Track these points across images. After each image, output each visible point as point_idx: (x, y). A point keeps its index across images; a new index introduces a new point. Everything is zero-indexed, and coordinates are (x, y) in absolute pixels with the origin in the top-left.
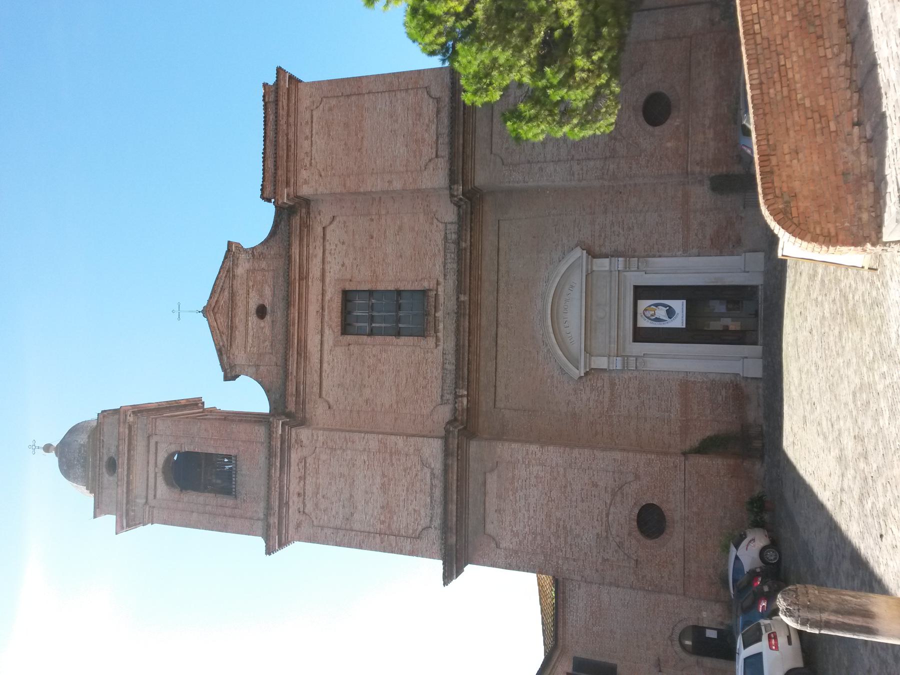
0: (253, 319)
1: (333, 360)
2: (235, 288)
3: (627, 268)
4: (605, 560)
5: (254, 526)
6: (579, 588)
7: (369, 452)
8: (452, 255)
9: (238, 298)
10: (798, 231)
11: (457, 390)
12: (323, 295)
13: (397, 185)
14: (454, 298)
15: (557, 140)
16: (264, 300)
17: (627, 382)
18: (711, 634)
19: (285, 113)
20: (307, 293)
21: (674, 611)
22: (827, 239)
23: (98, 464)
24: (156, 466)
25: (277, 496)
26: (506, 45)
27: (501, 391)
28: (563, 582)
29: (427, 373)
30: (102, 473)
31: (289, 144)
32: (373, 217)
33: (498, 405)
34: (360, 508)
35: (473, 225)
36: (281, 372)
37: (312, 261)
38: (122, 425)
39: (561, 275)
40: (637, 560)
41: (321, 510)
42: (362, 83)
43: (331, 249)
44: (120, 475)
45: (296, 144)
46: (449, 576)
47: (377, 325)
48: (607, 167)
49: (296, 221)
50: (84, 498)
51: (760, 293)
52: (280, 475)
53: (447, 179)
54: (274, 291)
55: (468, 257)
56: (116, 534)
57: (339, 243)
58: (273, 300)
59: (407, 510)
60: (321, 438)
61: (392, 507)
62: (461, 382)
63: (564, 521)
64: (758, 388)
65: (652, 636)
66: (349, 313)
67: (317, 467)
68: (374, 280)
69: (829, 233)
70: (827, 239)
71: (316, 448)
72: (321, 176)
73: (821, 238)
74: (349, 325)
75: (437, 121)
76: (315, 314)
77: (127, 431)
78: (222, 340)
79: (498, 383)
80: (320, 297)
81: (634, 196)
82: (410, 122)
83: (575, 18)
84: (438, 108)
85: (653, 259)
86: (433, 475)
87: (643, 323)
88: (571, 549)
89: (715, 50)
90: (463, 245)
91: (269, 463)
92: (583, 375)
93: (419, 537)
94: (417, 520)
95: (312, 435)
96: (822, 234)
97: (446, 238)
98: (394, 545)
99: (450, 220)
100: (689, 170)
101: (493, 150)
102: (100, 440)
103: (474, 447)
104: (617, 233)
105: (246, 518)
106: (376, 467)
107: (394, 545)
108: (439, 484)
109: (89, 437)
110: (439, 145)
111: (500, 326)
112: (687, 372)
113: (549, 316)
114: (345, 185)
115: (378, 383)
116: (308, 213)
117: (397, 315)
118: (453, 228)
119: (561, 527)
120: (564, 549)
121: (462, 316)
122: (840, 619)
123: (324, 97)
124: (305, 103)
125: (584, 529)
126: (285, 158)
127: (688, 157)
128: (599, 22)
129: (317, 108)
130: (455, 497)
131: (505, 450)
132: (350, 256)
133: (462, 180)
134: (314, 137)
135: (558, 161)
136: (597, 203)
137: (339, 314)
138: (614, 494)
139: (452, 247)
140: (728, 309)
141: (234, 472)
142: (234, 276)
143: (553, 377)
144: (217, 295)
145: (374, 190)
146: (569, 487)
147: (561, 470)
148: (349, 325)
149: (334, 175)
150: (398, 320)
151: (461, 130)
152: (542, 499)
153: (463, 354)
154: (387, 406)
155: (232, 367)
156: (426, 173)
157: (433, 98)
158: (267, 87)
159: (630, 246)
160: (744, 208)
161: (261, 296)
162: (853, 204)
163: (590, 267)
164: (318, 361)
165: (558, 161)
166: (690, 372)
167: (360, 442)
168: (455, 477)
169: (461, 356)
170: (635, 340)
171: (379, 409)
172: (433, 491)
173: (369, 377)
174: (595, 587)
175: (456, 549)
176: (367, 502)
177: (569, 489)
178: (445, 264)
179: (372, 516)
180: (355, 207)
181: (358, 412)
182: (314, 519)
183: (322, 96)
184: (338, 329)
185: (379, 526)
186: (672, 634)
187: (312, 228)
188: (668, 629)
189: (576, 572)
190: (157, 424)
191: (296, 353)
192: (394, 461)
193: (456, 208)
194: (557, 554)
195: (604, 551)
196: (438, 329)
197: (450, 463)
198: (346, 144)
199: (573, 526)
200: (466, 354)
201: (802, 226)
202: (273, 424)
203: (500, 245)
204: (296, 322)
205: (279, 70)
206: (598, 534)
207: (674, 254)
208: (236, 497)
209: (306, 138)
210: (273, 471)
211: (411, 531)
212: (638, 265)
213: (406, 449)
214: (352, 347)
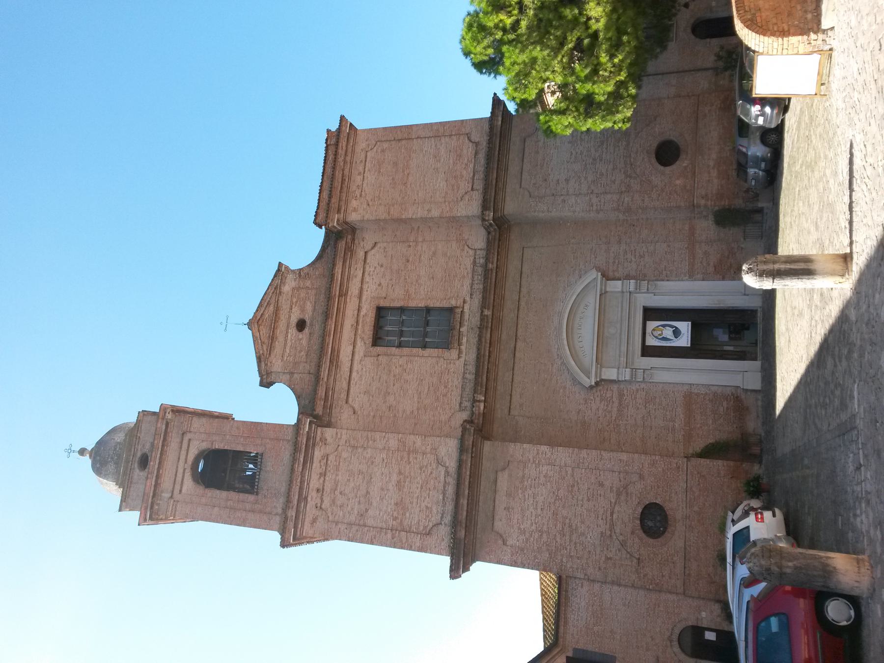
0: (293, 331)
1: (362, 369)
2: (280, 304)
3: (638, 288)
4: (608, 559)
5: (272, 521)
6: (582, 587)
7: (388, 450)
8: (479, 277)
9: (281, 312)
10: (761, 30)
11: (476, 395)
12: (359, 310)
13: (435, 213)
14: (478, 315)
15: (582, 133)
16: (305, 315)
17: (635, 394)
18: (710, 636)
19: (343, 153)
20: (345, 308)
21: (674, 611)
22: (782, 33)
23: (131, 459)
24: (186, 462)
25: (297, 490)
26: (544, 46)
27: (516, 398)
28: (566, 581)
29: (448, 382)
30: (134, 469)
31: (344, 178)
32: (411, 244)
33: (512, 412)
34: (375, 504)
35: (500, 250)
36: (313, 379)
37: (352, 280)
38: (160, 420)
39: (577, 293)
40: (639, 559)
41: (337, 506)
42: (412, 131)
43: (370, 271)
44: (151, 468)
45: (350, 179)
46: (456, 571)
47: (406, 339)
48: (623, 200)
49: (342, 245)
50: (112, 492)
51: (760, 315)
52: (302, 471)
53: (480, 209)
54: (315, 307)
55: (494, 277)
56: (139, 525)
57: (377, 266)
58: (313, 314)
59: (420, 507)
60: (344, 437)
61: (405, 504)
62: (479, 388)
63: (570, 520)
64: (757, 400)
65: (652, 637)
66: (381, 328)
67: (337, 464)
68: (407, 298)
69: (783, 29)
70: (782, 33)
71: (339, 446)
72: (369, 205)
73: (778, 33)
74: (380, 338)
75: (475, 161)
76: (350, 327)
77: (164, 427)
78: (263, 349)
79: (514, 392)
80: (356, 312)
81: (646, 228)
82: (451, 161)
83: (601, 25)
84: (476, 151)
85: (662, 282)
86: (447, 473)
87: (651, 342)
88: (575, 547)
89: (719, 106)
90: (490, 266)
91: (293, 458)
92: (593, 384)
93: (429, 534)
94: (428, 516)
95: (337, 434)
96: (778, 31)
97: (474, 262)
98: (404, 541)
99: (480, 247)
100: (695, 202)
101: (522, 184)
102: (137, 436)
103: (487, 446)
104: (629, 260)
105: (265, 513)
106: (393, 465)
107: (404, 541)
108: (452, 481)
109: (126, 435)
110: (475, 181)
111: (518, 340)
112: (691, 384)
113: (565, 330)
114: (389, 213)
115: (401, 391)
116: (353, 240)
117: (425, 330)
118: (483, 253)
119: (567, 525)
120: (569, 547)
121: (485, 328)
122: (788, 266)
123: (379, 141)
124: (361, 145)
125: (589, 527)
126: (339, 189)
127: (694, 193)
128: (620, 32)
129: (371, 149)
130: (467, 492)
131: (517, 450)
132: (386, 277)
133: (494, 208)
134: (366, 172)
135: (579, 194)
136: (612, 234)
137: (372, 328)
138: (619, 494)
139: (480, 270)
140: (730, 338)
141: (259, 463)
142: (280, 292)
143: (565, 388)
144: (263, 309)
145: (414, 217)
146: (576, 486)
147: (569, 470)
148: (380, 338)
149: (380, 204)
150: (426, 335)
151: (496, 166)
152: (550, 498)
153: (483, 363)
154: (408, 413)
155: (268, 374)
156: (461, 203)
157: (473, 143)
158: (330, 133)
159: (641, 271)
160: (744, 239)
161: (303, 310)
162: (800, 10)
163: (603, 288)
164: (348, 370)
165: (579, 194)
166: (693, 384)
167: (380, 440)
168: (468, 473)
169: (481, 364)
170: (643, 355)
171: (400, 415)
172: (446, 489)
173: (394, 385)
174: (597, 586)
175: (465, 544)
176: (382, 499)
177: (576, 488)
178: (472, 285)
179: (386, 512)
180: (396, 235)
181: (381, 417)
182: (330, 514)
183: (377, 140)
184: (369, 341)
185: (391, 523)
186: (672, 635)
187: (355, 253)
188: (668, 630)
189: (579, 570)
190: (193, 422)
191: (328, 360)
192: (411, 460)
193: (487, 234)
194: (562, 552)
195: (608, 549)
196: (462, 343)
197: (465, 458)
198: (393, 179)
199: (579, 524)
200: (486, 363)
201: (764, 27)
202: (302, 422)
203: (523, 269)
204: (332, 333)
205: (342, 118)
206: (602, 533)
207: (681, 279)
208: (257, 494)
209: (359, 174)
210: (297, 466)
211: (421, 528)
212: (648, 287)
213: (424, 448)
214: (380, 358)
